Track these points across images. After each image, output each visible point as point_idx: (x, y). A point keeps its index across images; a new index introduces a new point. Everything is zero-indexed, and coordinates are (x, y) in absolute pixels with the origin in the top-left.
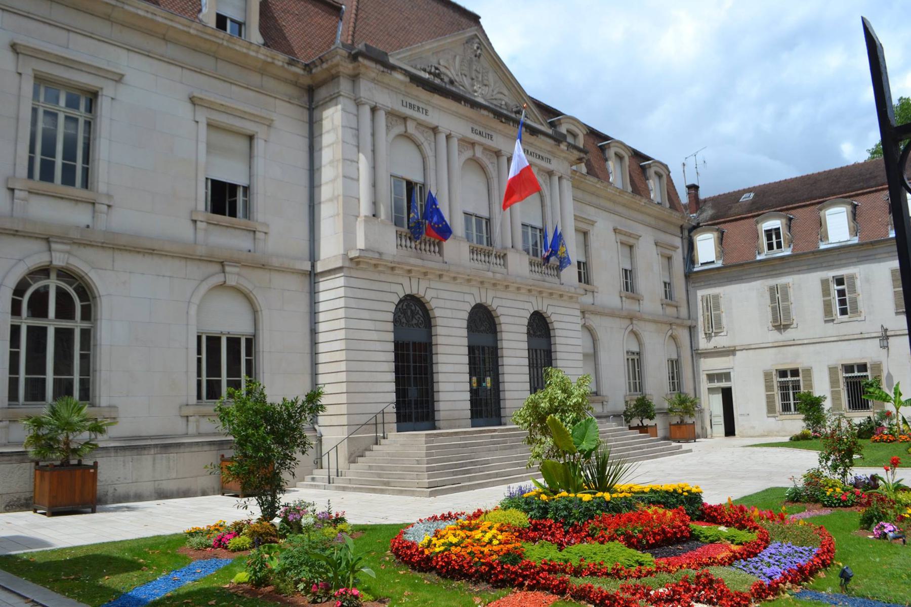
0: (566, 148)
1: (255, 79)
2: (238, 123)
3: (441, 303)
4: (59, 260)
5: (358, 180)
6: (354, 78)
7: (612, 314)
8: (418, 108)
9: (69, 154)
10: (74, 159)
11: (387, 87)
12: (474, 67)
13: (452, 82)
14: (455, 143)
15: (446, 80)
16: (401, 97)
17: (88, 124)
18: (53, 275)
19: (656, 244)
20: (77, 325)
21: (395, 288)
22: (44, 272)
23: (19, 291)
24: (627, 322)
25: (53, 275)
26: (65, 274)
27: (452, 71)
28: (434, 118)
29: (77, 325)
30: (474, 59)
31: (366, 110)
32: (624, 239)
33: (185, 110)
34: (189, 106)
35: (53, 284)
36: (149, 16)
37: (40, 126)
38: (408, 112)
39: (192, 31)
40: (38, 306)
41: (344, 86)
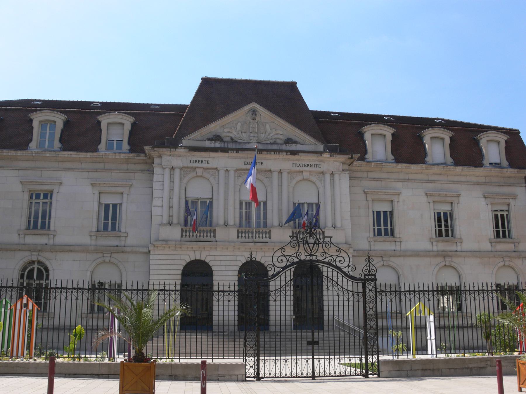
0: (329, 156)
1: (125, 166)
2: (113, 189)
3: (218, 263)
4: (34, 258)
5: (162, 206)
6: (160, 156)
7: (416, 254)
8: (202, 161)
9: (44, 216)
10: (38, 218)
11: (179, 156)
12: (251, 126)
13: (232, 140)
14: (232, 173)
15: (225, 139)
16: (190, 158)
17: (51, 203)
18: (36, 263)
19: (485, 197)
20: (43, 282)
21: (182, 257)
22: (33, 262)
23: (24, 269)
24: (439, 260)
25: (36, 263)
26: (40, 263)
27: (235, 133)
28: (213, 163)
29: (43, 282)
30: (251, 121)
31: (167, 171)
32: (437, 199)
33: (89, 189)
34: (91, 187)
35: (36, 266)
36: (69, 156)
37: (33, 208)
38: (195, 165)
39: (88, 156)
40: (30, 276)
41: (157, 160)
